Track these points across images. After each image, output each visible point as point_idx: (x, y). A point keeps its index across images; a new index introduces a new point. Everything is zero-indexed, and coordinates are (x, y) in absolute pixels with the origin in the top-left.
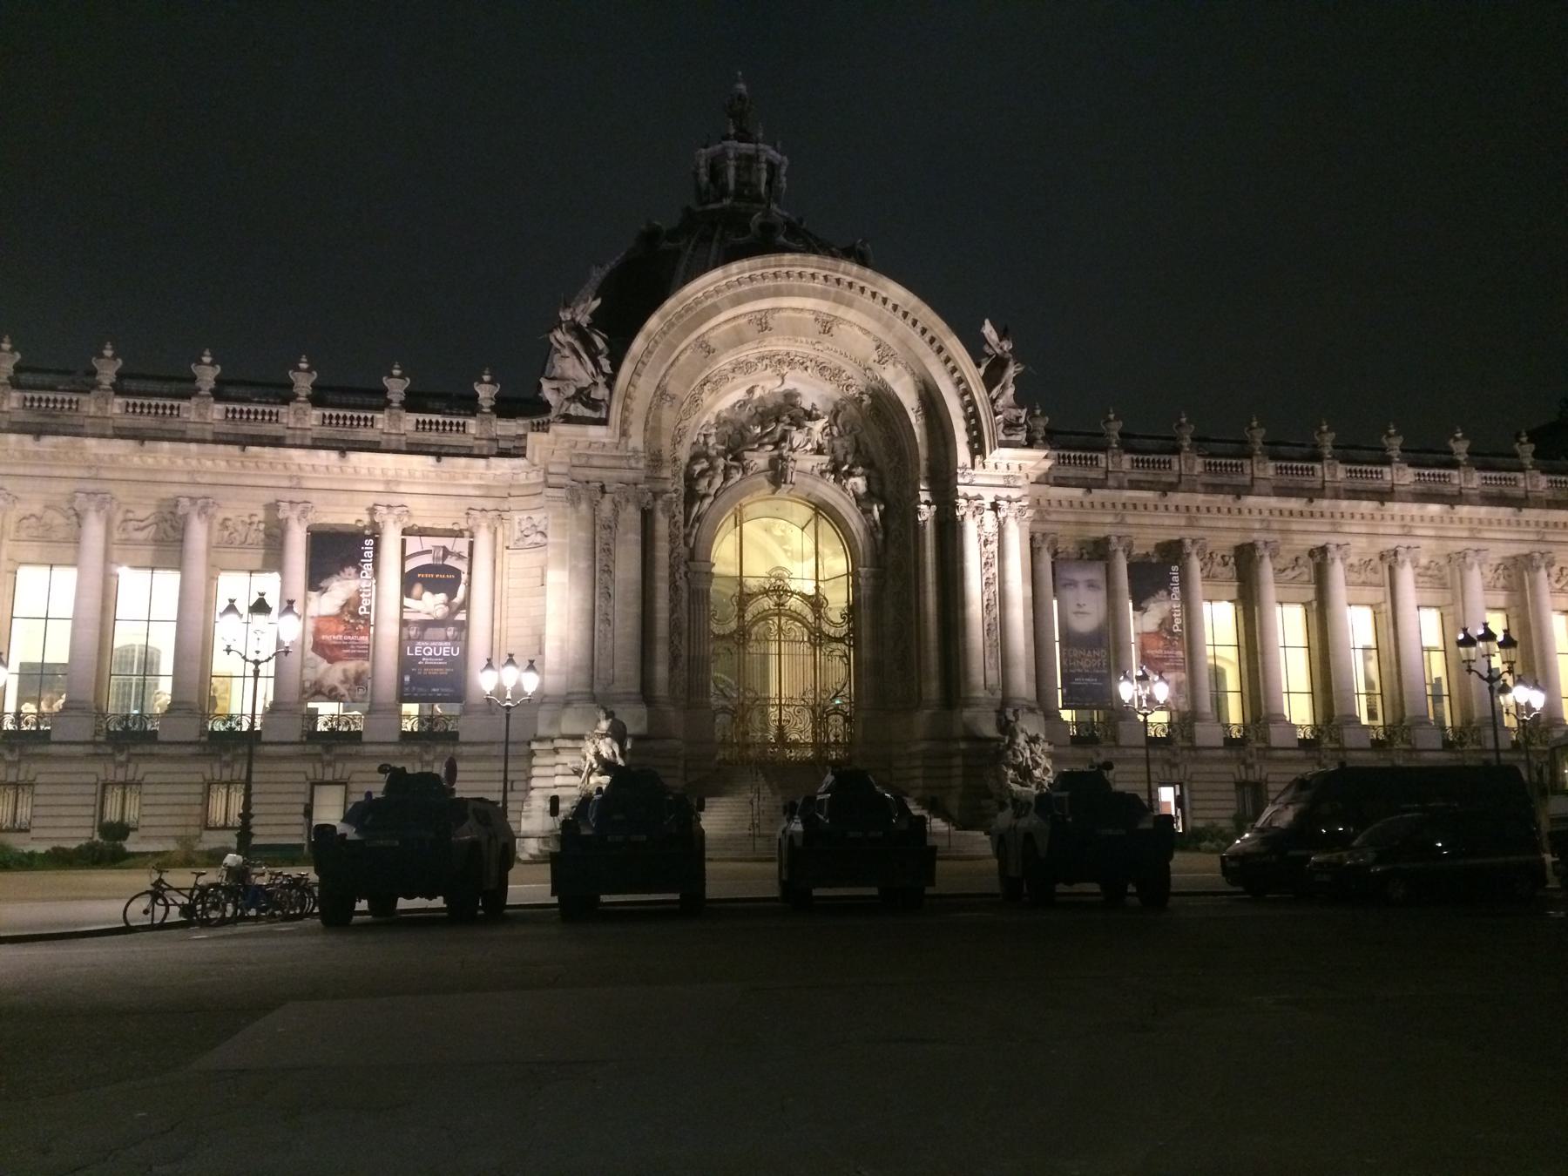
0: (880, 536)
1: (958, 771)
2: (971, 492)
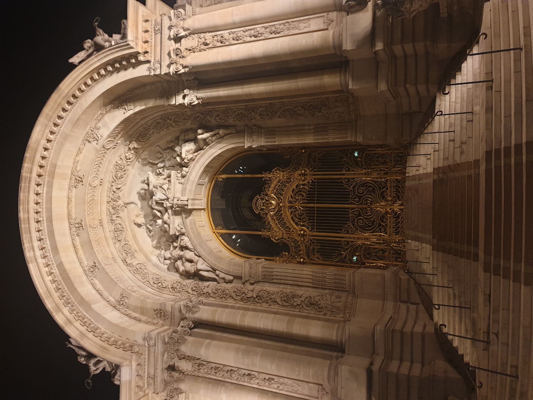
0: (221, 132)
1: (409, 48)
2: (166, 61)
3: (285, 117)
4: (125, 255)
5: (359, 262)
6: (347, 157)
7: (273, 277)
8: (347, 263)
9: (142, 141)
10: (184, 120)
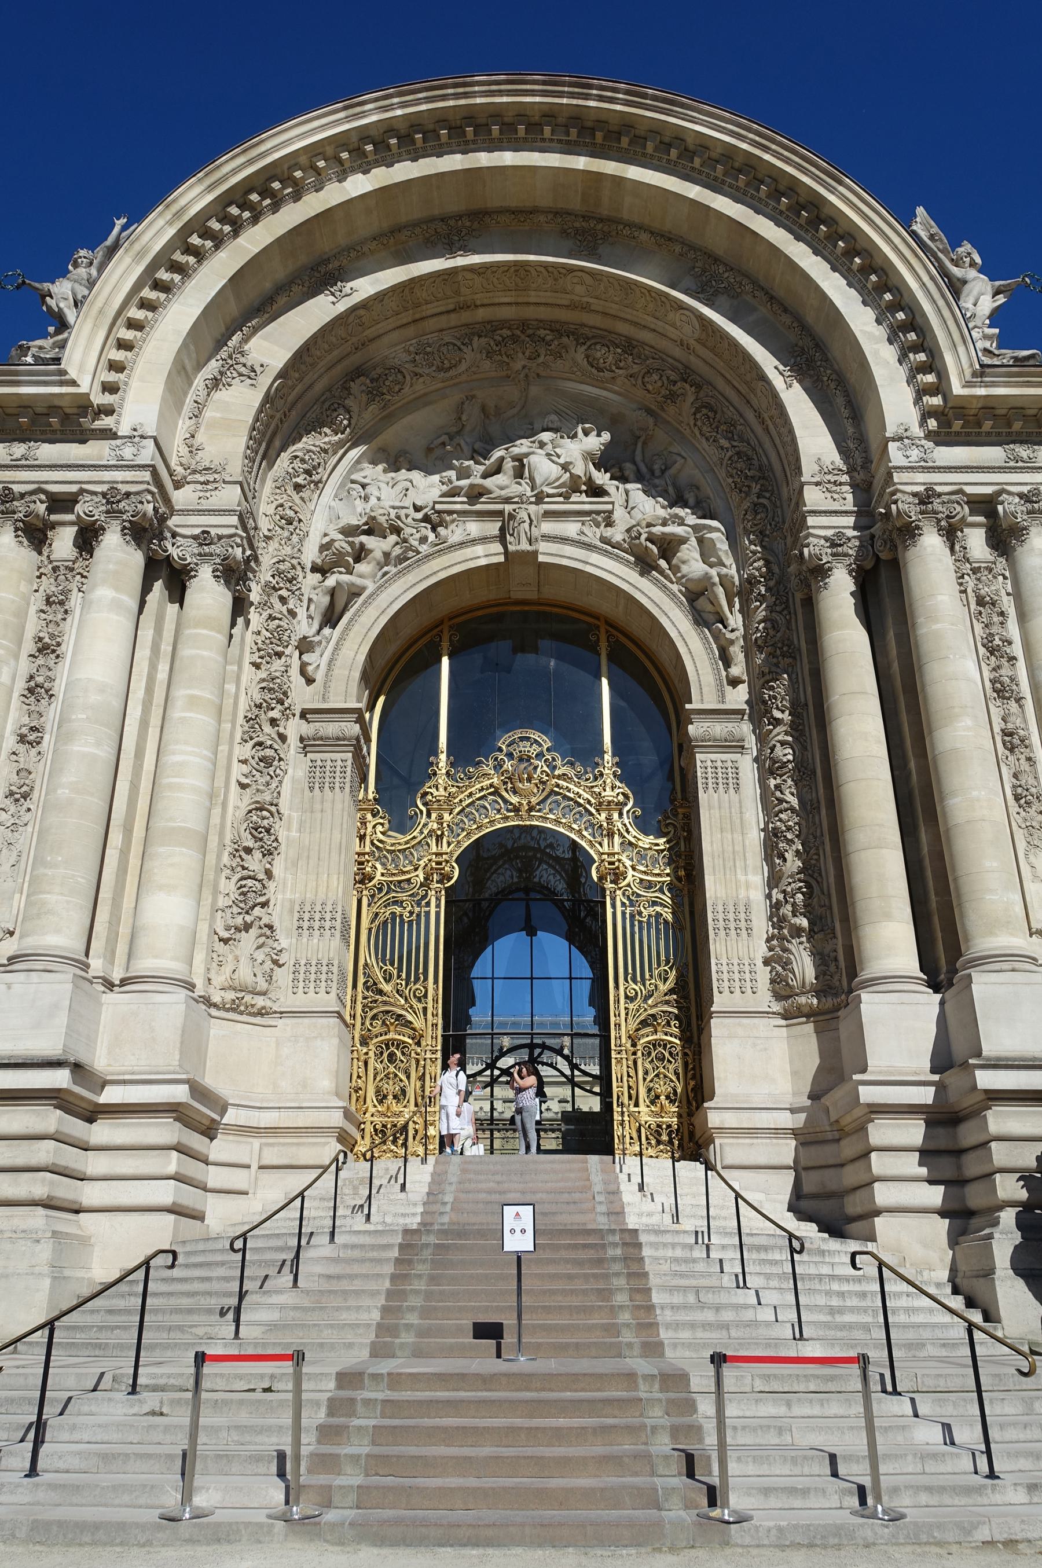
5: (369, 1030)
6: (666, 995)
8: (365, 998)
9: (698, 416)
10: (761, 532)
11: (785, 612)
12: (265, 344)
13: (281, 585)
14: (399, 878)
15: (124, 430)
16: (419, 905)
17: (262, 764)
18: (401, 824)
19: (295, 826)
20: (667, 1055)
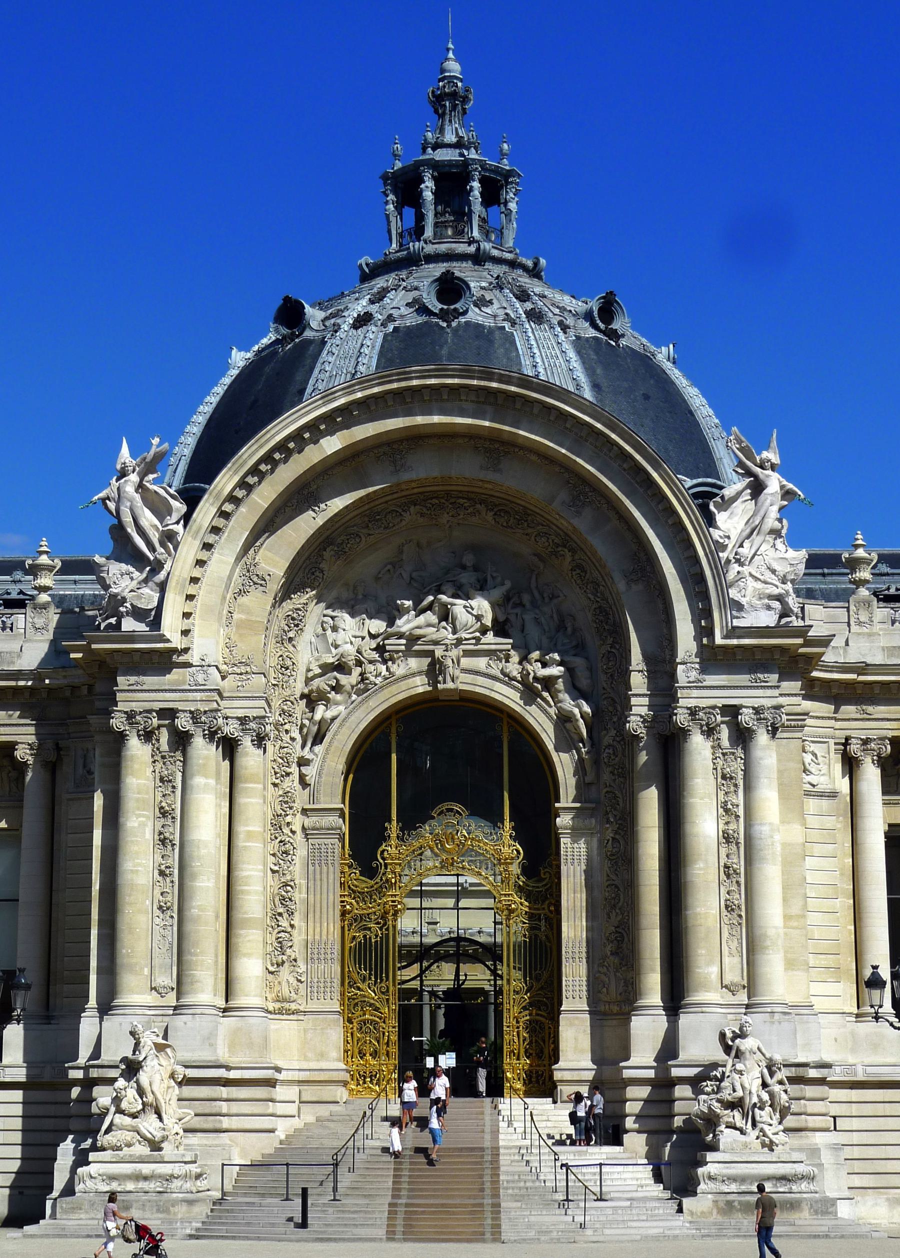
3: (607, 887)
4: (339, 541)
5: (353, 1014)
6: (539, 990)
7: (317, 865)
9: (574, 573)
11: (622, 743)
12: (269, 554)
13: (286, 721)
14: (368, 912)
15: (195, 660)
16: (381, 929)
17: (284, 855)
18: (369, 872)
19: (304, 890)
20: (538, 1028)
